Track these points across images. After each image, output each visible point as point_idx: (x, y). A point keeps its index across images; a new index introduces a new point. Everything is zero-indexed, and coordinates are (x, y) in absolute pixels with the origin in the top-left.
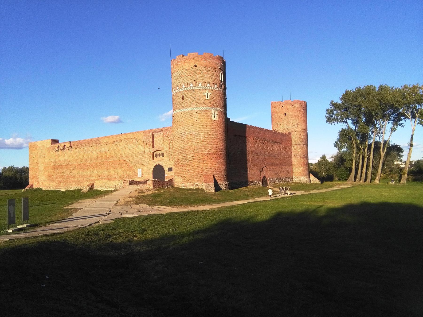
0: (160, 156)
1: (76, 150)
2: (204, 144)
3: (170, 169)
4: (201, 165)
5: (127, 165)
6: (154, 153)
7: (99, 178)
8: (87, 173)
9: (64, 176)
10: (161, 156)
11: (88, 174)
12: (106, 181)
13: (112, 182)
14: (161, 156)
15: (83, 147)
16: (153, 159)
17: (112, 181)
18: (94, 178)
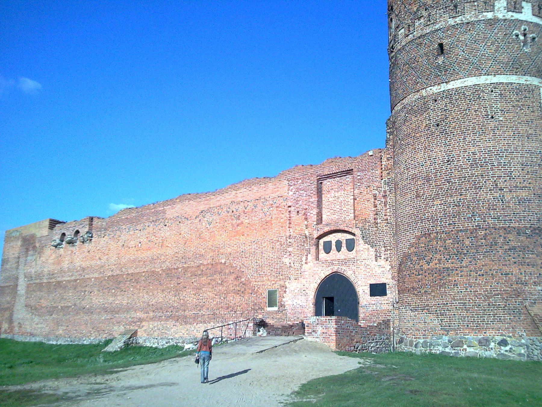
0: (339, 249)
1: (103, 241)
2: (524, 194)
3: (378, 290)
4: (515, 270)
5: (234, 276)
6: (321, 241)
7: (151, 314)
8: (122, 300)
9: (68, 307)
10: (344, 248)
11: (125, 303)
12: (170, 323)
13: (188, 326)
14: (344, 248)
15: (118, 233)
16: (317, 258)
17: (186, 323)
18: (139, 315)
